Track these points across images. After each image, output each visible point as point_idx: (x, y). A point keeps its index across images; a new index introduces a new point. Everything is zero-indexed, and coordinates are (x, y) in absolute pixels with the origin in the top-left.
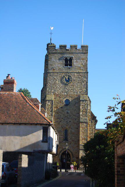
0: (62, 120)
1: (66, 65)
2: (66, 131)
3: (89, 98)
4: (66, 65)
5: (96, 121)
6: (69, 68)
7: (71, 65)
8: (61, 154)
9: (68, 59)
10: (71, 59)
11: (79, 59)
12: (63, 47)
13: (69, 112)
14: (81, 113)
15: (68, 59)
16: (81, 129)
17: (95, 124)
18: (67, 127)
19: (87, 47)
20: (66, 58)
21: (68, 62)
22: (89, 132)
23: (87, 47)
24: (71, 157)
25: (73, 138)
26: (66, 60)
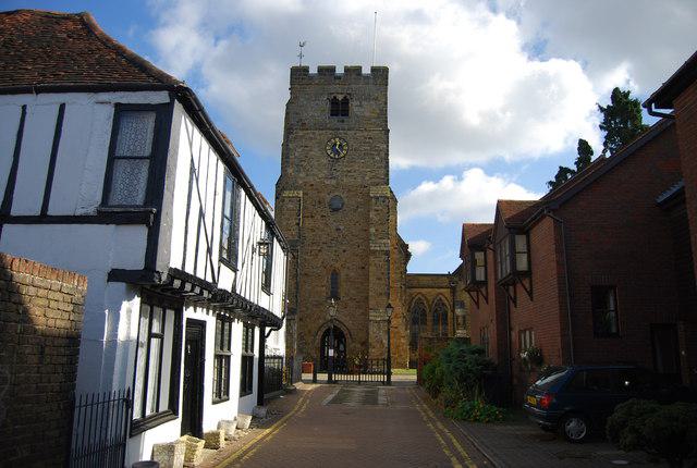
0: (325, 246)
1: (334, 113)
2: (335, 275)
3: (391, 192)
4: (334, 113)
5: (408, 256)
6: (343, 121)
7: (345, 113)
8: (321, 333)
9: (340, 97)
10: (346, 102)
11: (365, 99)
12: (327, 72)
13: (342, 228)
14: (373, 230)
15: (340, 97)
16: (372, 269)
17: (406, 264)
18: (337, 265)
19: (386, 70)
20: (335, 97)
21: (340, 108)
22: (392, 276)
23: (386, 70)
24: (349, 341)
25: (352, 291)
26: (334, 102)
